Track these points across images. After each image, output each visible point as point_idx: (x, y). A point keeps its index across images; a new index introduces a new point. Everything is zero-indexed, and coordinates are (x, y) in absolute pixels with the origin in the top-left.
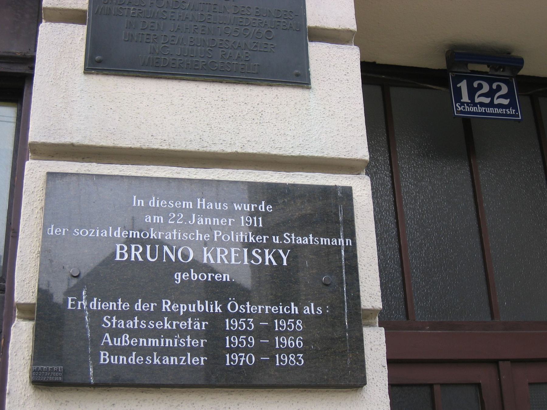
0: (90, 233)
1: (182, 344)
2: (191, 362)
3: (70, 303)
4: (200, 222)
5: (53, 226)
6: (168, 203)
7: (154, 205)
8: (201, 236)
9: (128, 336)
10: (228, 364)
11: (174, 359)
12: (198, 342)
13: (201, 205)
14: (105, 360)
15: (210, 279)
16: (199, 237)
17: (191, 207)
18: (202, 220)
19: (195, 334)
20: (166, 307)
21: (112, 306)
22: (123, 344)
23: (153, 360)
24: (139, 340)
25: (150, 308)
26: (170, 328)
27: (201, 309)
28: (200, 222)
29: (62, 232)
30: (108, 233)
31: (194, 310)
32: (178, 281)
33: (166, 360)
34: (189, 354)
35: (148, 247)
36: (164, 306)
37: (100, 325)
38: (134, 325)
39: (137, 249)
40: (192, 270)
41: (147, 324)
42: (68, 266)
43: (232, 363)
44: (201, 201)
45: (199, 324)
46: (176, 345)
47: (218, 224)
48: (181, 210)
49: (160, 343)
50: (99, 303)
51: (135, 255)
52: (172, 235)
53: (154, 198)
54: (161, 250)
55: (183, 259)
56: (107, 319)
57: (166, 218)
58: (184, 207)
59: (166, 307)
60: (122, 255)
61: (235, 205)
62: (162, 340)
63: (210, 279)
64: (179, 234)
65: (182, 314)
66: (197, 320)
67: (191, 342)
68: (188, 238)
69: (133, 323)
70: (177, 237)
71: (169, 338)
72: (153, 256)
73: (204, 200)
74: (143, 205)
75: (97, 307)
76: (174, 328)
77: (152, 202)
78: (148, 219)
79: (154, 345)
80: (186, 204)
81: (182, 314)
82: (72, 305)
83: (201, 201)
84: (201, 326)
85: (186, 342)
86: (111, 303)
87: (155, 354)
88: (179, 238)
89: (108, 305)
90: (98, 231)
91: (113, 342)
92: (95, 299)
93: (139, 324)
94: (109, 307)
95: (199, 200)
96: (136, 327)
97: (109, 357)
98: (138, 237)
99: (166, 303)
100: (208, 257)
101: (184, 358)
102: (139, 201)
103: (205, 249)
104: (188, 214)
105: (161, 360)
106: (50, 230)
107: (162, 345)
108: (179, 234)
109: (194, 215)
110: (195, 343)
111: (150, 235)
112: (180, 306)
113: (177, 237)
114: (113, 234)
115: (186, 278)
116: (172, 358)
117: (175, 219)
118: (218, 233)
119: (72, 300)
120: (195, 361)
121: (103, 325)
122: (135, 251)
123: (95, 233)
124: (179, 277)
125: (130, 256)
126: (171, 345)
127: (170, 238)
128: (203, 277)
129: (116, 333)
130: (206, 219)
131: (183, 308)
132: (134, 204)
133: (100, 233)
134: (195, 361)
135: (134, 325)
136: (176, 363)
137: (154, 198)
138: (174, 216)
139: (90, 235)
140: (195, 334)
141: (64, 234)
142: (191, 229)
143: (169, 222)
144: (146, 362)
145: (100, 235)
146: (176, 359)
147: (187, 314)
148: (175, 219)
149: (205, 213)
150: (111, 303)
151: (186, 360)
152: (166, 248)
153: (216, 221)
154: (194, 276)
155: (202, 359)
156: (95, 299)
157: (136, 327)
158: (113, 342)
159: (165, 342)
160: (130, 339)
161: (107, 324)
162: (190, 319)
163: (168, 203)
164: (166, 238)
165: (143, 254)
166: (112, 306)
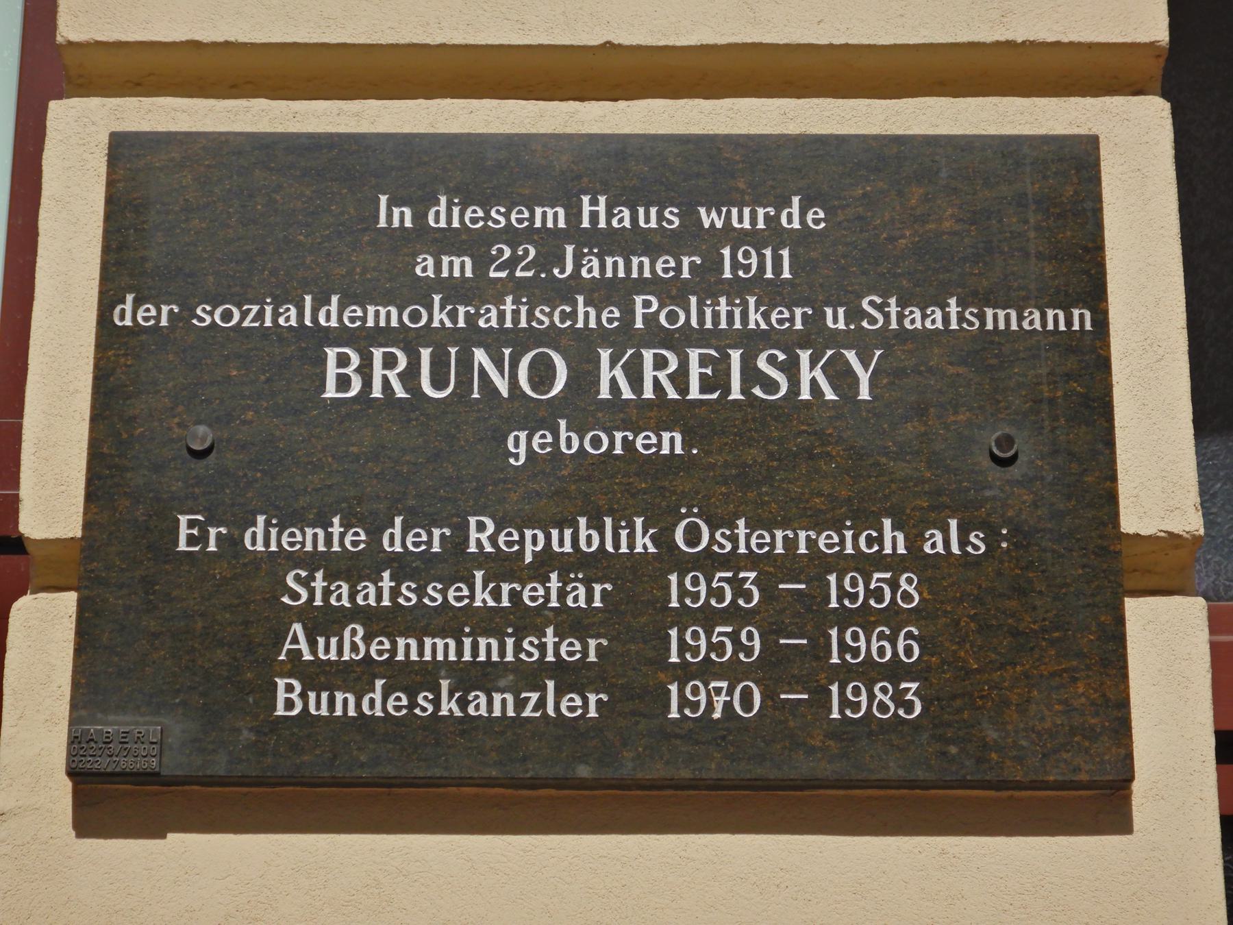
0: (244, 315)
1: (530, 655)
3: (184, 532)
6: (487, 213)
9: (361, 632)
11: (504, 701)
13: (594, 216)
15: (618, 451)
16: (586, 315)
19: (573, 624)
20: (478, 540)
21: (310, 538)
22: (346, 658)
23: (437, 703)
24: (394, 644)
27: (589, 544)
30: (301, 315)
31: (568, 548)
32: (516, 457)
33: (479, 705)
34: (551, 685)
35: (426, 354)
36: (473, 535)
37: (277, 599)
38: (379, 597)
39: (390, 362)
40: (563, 424)
41: (421, 592)
43: (687, 712)
44: (594, 202)
45: (582, 591)
46: (509, 658)
48: (530, 234)
50: (274, 531)
51: (386, 380)
52: (501, 316)
54: (466, 362)
55: (534, 389)
56: (297, 578)
57: (481, 265)
59: (478, 540)
62: (467, 642)
63: (618, 451)
64: (524, 309)
65: (528, 558)
66: (576, 580)
67: (557, 646)
68: (552, 322)
69: (376, 592)
73: (602, 200)
74: (408, 224)
75: (267, 543)
76: (505, 603)
78: (425, 267)
82: (191, 540)
83: (594, 202)
84: (590, 598)
89: (299, 539)
90: (269, 310)
92: (261, 519)
93: (395, 593)
94: (303, 544)
95: (586, 199)
97: (303, 695)
98: (394, 323)
99: (481, 527)
101: (534, 696)
102: (396, 211)
105: (463, 703)
109: (570, 249)
110: (569, 649)
112: (522, 536)
113: (516, 320)
114: (315, 319)
115: (542, 446)
117: (511, 264)
118: (647, 304)
119: (191, 524)
120: (571, 705)
121: (286, 600)
123: (260, 315)
124: (520, 446)
128: (596, 442)
129: (324, 622)
130: (609, 261)
131: (535, 543)
132: (382, 223)
133: (276, 314)
134: (571, 705)
135: (379, 597)
138: (507, 253)
139: (246, 324)
140: (573, 624)
142: (563, 292)
143: (492, 274)
144: (417, 711)
145: (275, 321)
146: (510, 698)
147: (546, 561)
148: (511, 264)
150: (309, 532)
151: (541, 704)
154: (569, 439)
155: (592, 698)
156: (261, 519)
158: (314, 651)
160: (367, 639)
161: (295, 596)
162: (554, 576)
163: (487, 213)
164: (481, 323)
165: (410, 376)
166: (310, 538)
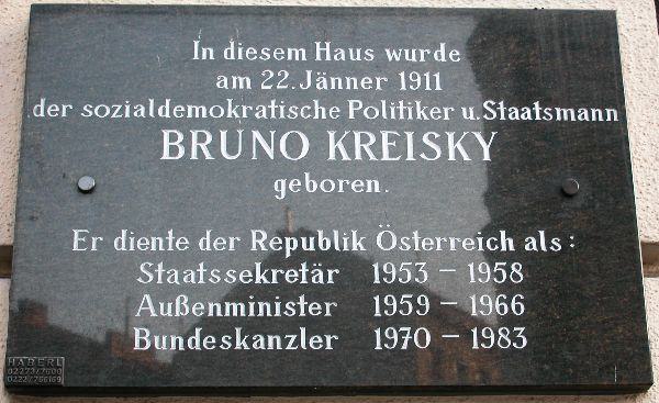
0: (112, 111)
1: (290, 312)
2: (307, 344)
3: (76, 239)
4: (321, 85)
5: (42, 101)
6: (259, 52)
7: (232, 57)
8: (323, 109)
9: (186, 300)
10: (378, 347)
11: (275, 340)
12: (319, 307)
13: (323, 54)
14: (143, 343)
15: (341, 190)
16: (320, 111)
17: (304, 58)
18: (325, 80)
19: (316, 293)
20: (257, 244)
21: (155, 243)
22: (177, 315)
23: (233, 341)
24: (207, 306)
25: (228, 245)
26: (266, 281)
27: (325, 246)
28: (321, 85)
29: (60, 112)
30: (147, 110)
31: (312, 248)
32: (279, 194)
33: (260, 342)
34: (303, 330)
35: (223, 134)
36: (254, 241)
37: (134, 279)
38: (197, 279)
39: (202, 138)
40: (307, 175)
41: (222, 274)
42: (72, 173)
43: (386, 345)
44: (323, 46)
45: (321, 274)
46: (278, 314)
47: (355, 87)
48: (285, 64)
49: (247, 311)
50: (132, 240)
51: (199, 149)
52: (269, 111)
53: (232, 44)
54: (248, 139)
55: (289, 153)
56: (146, 267)
57: (256, 82)
58: (290, 58)
59: (257, 244)
60: (173, 151)
61: (388, 51)
62: (252, 305)
63: (341, 190)
64: (282, 108)
65: (288, 255)
66: (317, 267)
67: (306, 308)
68: (299, 116)
69: (197, 275)
70: (277, 114)
71: (263, 300)
72: (232, 150)
73: (328, 44)
74: (211, 57)
75: (128, 246)
76: (274, 281)
77: (229, 52)
78: (223, 82)
79: (235, 314)
80: (294, 52)
81: (288, 255)
82: (81, 244)
83: (323, 46)
84: (326, 278)
85: (297, 308)
86: (154, 239)
87: (238, 330)
88: (282, 116)
89: (148, 243)
90: (128, 108)
91: (157, 311)
92: (124, 232)
93: (207, 276)
94: (150, 246)
95: (318, 44)
96: (201, 281)
97: (151, 338)
98: (204, 116)
99: (259, 236)
100: (337, 150)
101: (294, 337)
102: (204, 50)
103: (332, 135)
104: (297, 69)
105: (250, 342)
106: (39, 108)
107: (252, 314)
108: (282, 108)
109: (309, 73)
110: (314, 308)
111: (226, 113)
112: (284, 241)
113: (277, 114)
114: (156, 113)
115: (295, 188)
116: (270, 338)
117: (274, 81)
118: (356, 105)
119: (81, 235)
120: (315, 342)
121: (140, 280)
122: (199, 141)
123: (122, 111)
124: (282, 188)
125: (188, 151)
126: (269, 314)
127: (264, 115)
128: (328, 186)
129: (164, 293)
130: (333, 80)
131: (292, 245)
132: (196, 57)
133: (132, 110)
134: (315, 342)
135: (197, 279)
136: (279, 347)
137: (232, 44)
138: (272, 75)
139: (114, 116)
140: (316, 293)
141: (64, 115)
142: (305, 98)
143: (263, 87)
144: (221, 347)
145: (131, 114)
146: (278, 339)
147: (299, 256)
148: (274, 81)
149: (331, 69)
150: (154, 239)
151: (298, 341)
152: (256, 135)
153: (352, 83)
154: (311, 184)
155: (329, 338)
156: (124, 232)
157: (201, 281)
158: (157, 311)
159: (256, 308)
160: (190, 304)
161: (146, 278)
162: (304, 265)
163: (259, 52)
164: (257, 115)
165: (214, 147)
166: (155, 243)
